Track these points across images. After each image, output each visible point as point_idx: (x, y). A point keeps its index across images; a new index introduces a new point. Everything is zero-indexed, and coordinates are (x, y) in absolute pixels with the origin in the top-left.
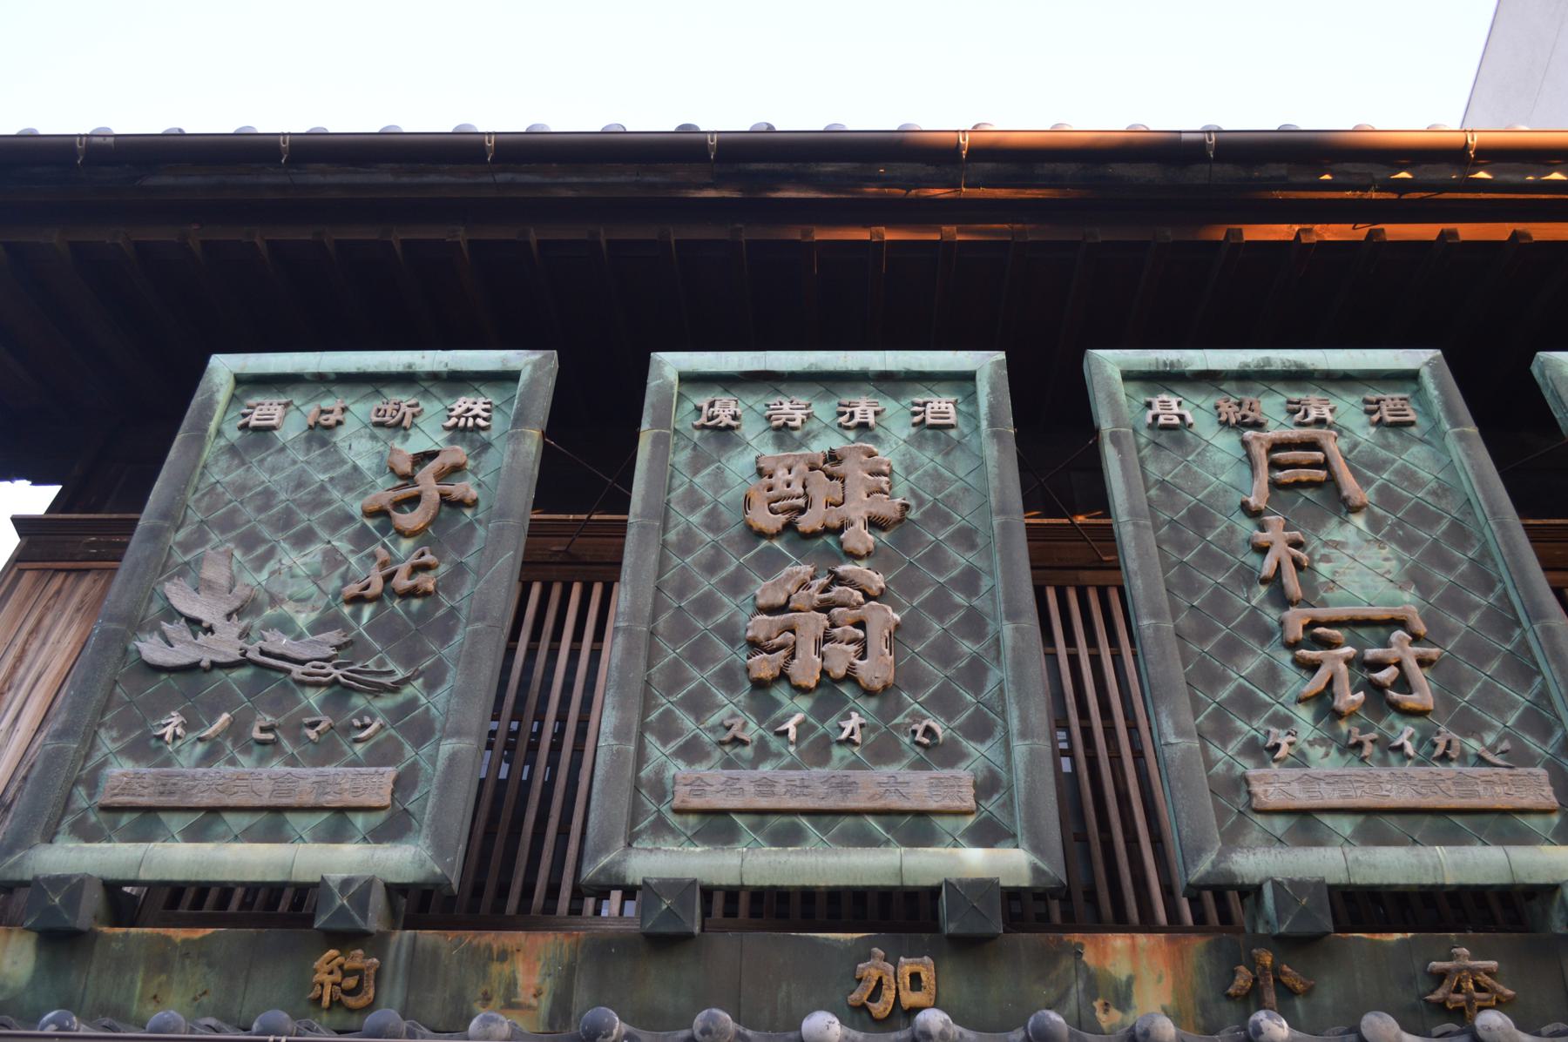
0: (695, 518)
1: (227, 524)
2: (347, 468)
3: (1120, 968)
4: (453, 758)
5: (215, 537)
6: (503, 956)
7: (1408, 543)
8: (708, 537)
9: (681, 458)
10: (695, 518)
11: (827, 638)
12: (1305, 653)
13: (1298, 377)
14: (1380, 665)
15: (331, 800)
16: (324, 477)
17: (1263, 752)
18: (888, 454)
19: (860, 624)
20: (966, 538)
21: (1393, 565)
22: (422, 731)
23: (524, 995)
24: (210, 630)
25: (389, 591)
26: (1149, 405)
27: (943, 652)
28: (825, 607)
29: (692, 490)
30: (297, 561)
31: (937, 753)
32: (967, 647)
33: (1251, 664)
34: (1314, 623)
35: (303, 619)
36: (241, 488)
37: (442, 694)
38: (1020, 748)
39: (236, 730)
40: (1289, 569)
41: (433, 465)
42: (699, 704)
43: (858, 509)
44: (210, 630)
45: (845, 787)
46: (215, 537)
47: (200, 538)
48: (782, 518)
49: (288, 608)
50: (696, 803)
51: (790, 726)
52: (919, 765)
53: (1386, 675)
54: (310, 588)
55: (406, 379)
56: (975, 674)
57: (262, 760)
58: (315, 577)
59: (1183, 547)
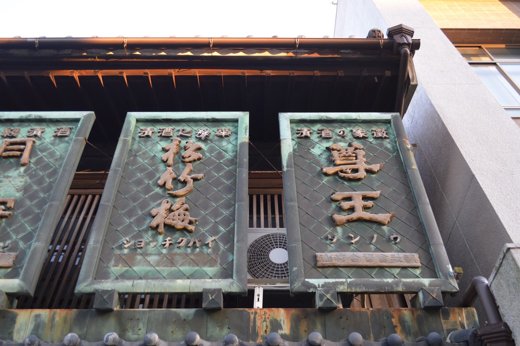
13: (40, 121)
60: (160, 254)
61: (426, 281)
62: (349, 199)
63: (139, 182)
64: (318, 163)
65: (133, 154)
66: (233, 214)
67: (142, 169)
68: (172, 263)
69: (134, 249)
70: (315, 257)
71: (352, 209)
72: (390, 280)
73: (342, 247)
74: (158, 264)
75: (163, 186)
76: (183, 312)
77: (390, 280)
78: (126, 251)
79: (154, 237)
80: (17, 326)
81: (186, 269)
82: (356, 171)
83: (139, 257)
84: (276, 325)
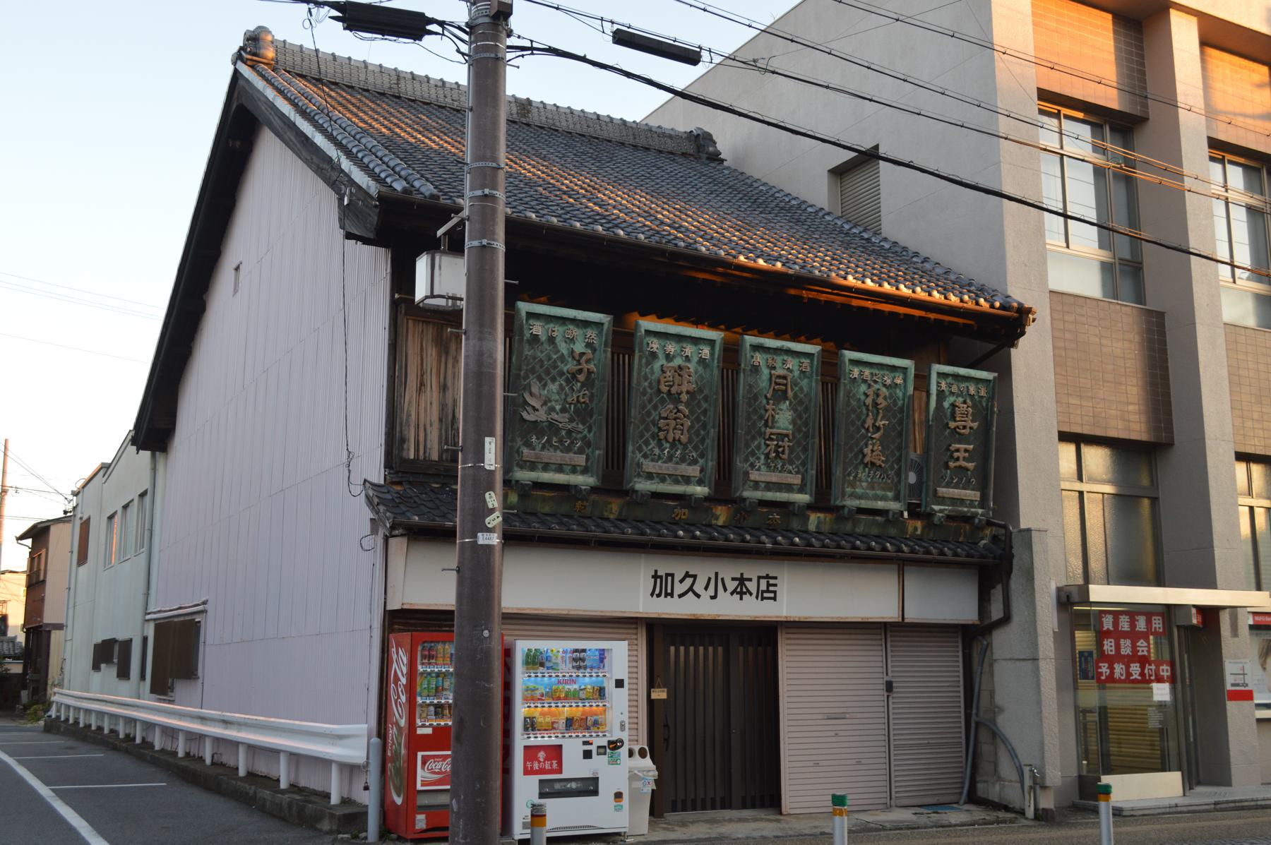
0: (646, 384)
1: (533, 371)
2: (560, 353)
3: (718, 513)
4: (599, 455)
5: (531, 377)
6: (610, 503)
7: (795, 411)
8: (649, 391)
9: (644, 360)
10: (646, 384)
11: (675, 429)
12: (768, 442)
13: (789, 352)
14: (780, 447)
15: (573, 463)
16: (555, 357)
17: (752, 466)
18: (692, 366)
19: (682, 425)
20: (706, 398)
21: (790, 417)
22: (588, 444)
23: (613, 511)
24: (537, 410)
25: (578, 401)
26: (753, 357)
27: (697, 434)
28: (675, 419)
29: (646, 374)
30: (554, 387)
31: (694, 462)
32: (702, 432)
33: (756, 443)
34: (772, 434)
35: (558, 407)
36: (534, 358)
37: (592, 434)
38: (710, 463)
39: (549, 441)
40: (770, 418)
41: (584, 358)
42: (647, 443)
43: (684, 388)
44: (537, 410)
45: (676, 469)
46: (531, 377)
47: (526, 377)
48: (668, 388)
49: (553, 403)
50: (647, 470)
51: (666, 452)
52: (689, 464)
53: (780, 450)
54: (558, 397)
55: (573, 321)
56: (703, 440)
57: (555, 450)
58: (558, 394)
59: (750, 406)
60: (867, 481)
61: (980, 511)
62: (958, 450)
63: (853, 423)
64: (945, 415)
65: (848, 394)
66: (901, 456)
67: (854, 411)
68: (873, 489)
69: (855, 477)
70: (936, 490)
71: (958, 459)
72: (966, 509)
73: (948, 485)
74: (867, 488)
75: (867, 430)
76: (878, 518)
77: (966, 509)
78: (851, 478)
79: (864, 468)
80: (810, 521)
81: (879, 492)
82: (964, 427)
83: (858, 483)
84: (916, 529)
